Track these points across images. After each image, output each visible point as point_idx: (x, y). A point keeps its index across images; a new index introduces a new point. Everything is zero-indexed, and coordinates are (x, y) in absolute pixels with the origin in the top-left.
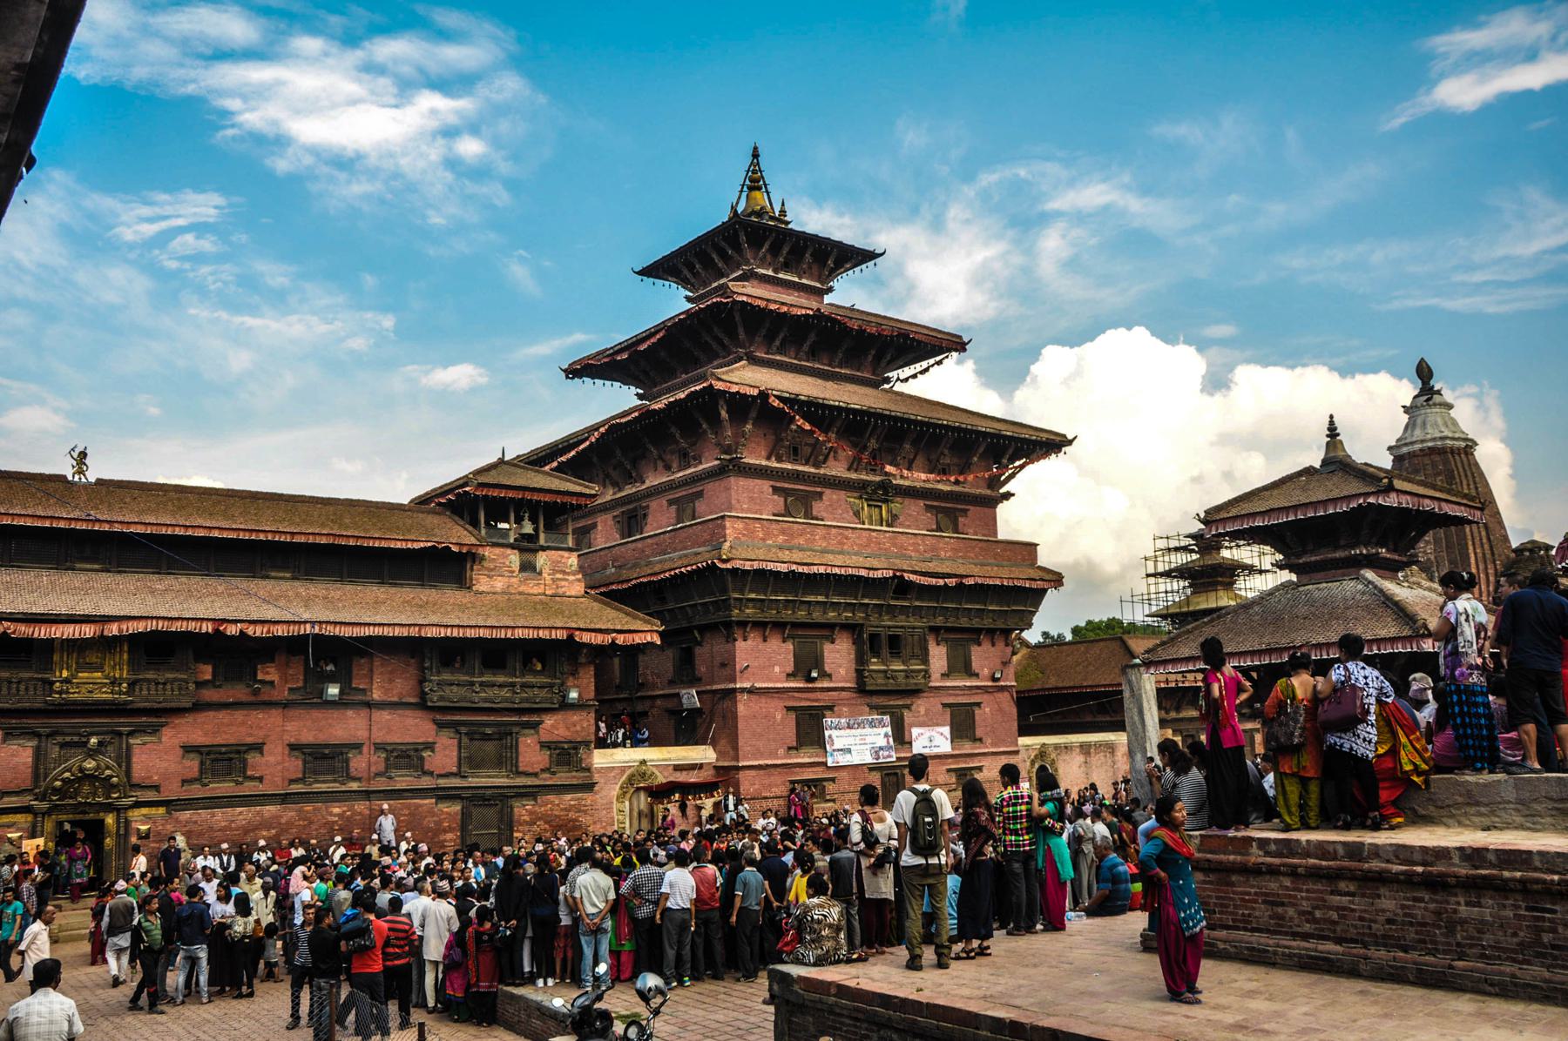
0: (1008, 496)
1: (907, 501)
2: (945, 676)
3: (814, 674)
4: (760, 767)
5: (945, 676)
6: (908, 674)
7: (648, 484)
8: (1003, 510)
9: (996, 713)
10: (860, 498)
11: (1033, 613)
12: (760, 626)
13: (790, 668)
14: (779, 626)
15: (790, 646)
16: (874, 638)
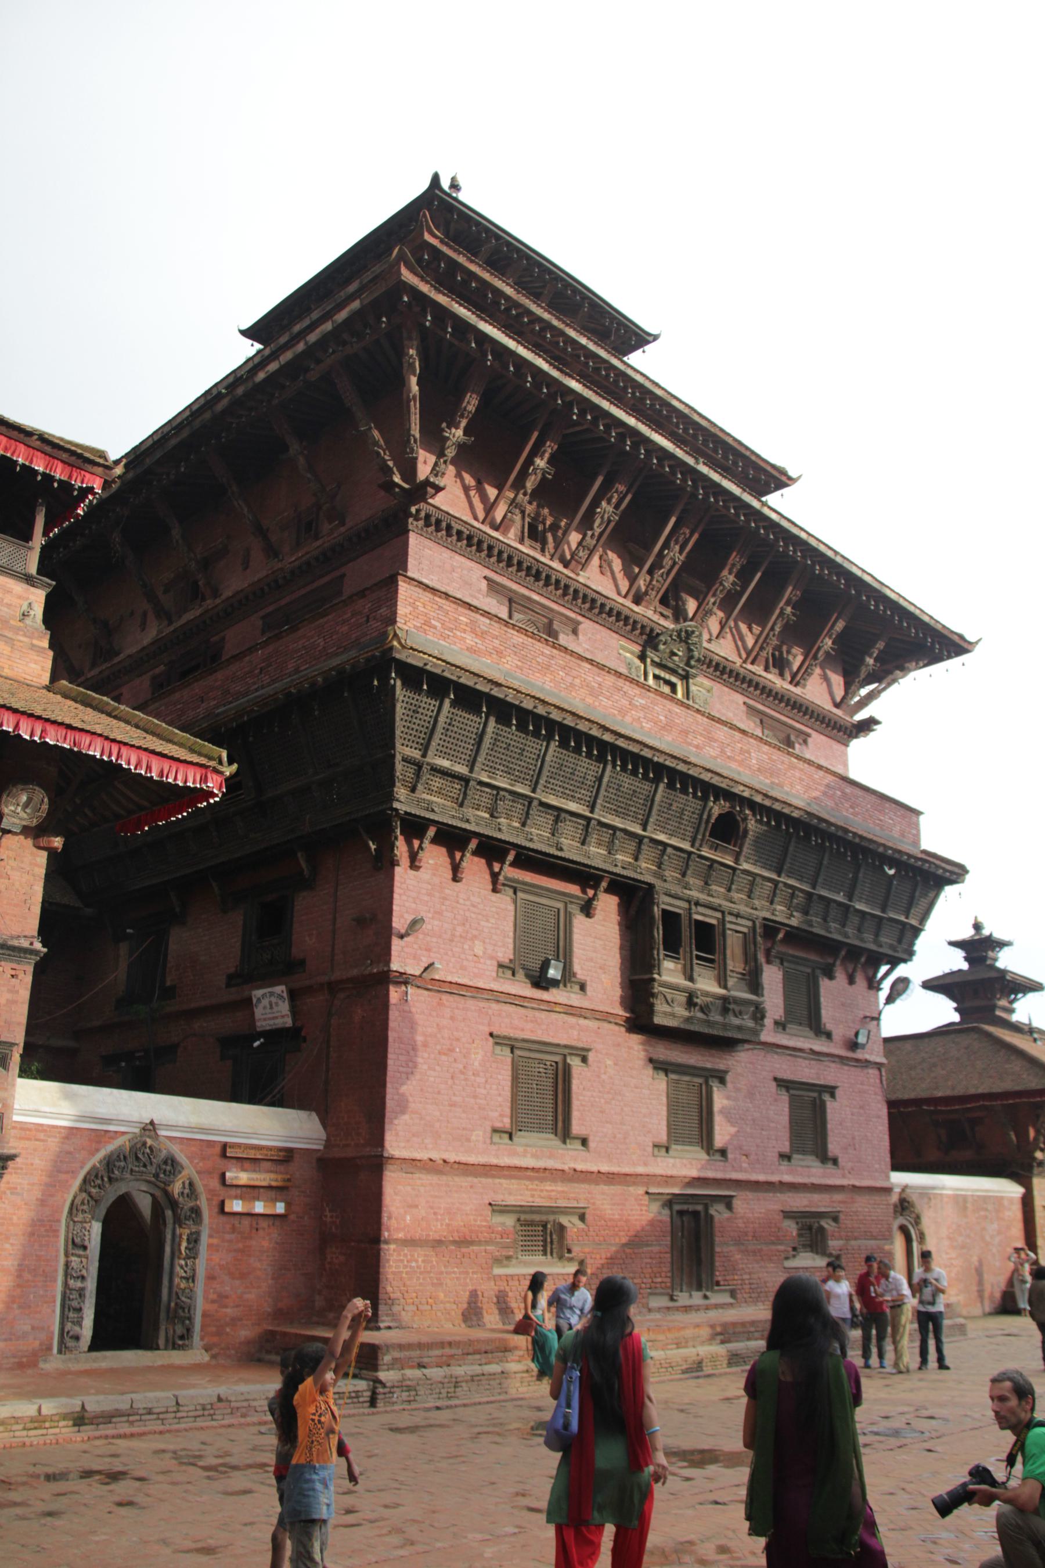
0: (868, 725)
1: (718, 688)
2: (780, 1025)
3: (553, 973)
4: (430, 1166)
5: (780, 1025)
6: (726, 1004)
7: (228, 593)
8: (857, 746)
9: (859, 1119)
10: (642, 657)
11: (916, 931)
12: (453, 839)
13: (506, 954)
14: (492, 850)
15: (504, 902)
16: (670, 919)
